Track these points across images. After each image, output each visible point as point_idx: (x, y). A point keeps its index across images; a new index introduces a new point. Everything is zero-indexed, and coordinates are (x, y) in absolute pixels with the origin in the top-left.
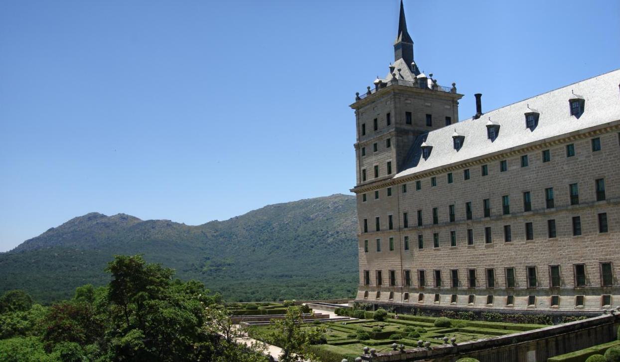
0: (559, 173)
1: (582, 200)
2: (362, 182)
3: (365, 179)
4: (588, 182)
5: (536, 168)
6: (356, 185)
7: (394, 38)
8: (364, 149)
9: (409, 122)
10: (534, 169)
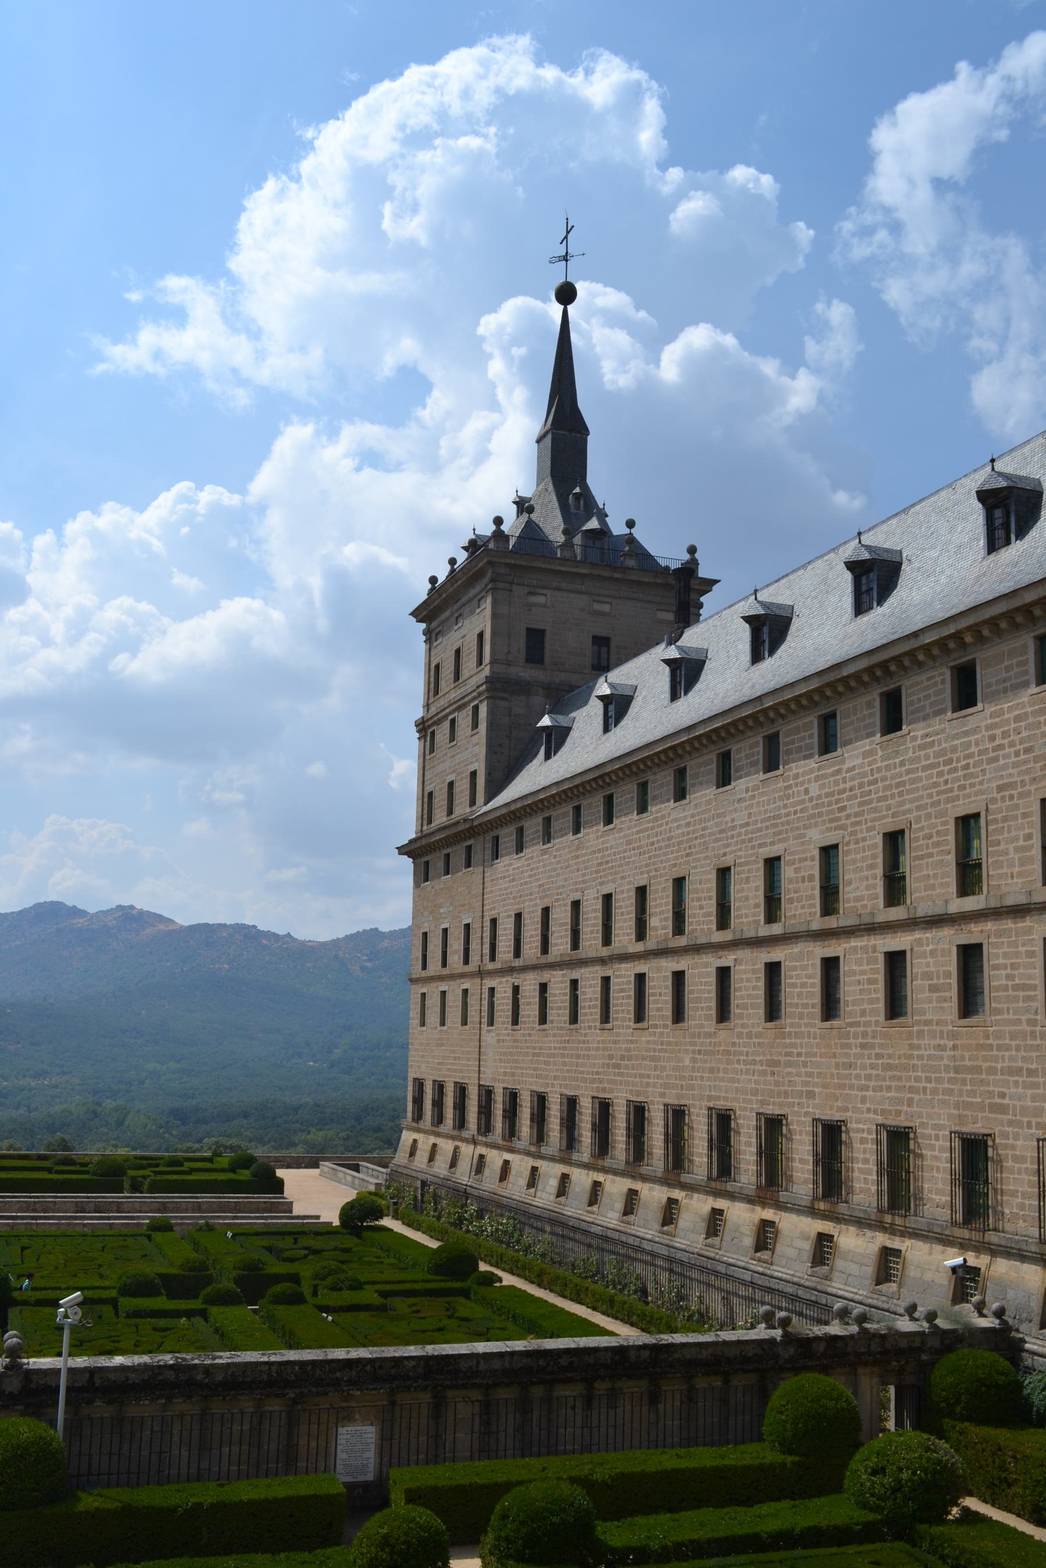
0: (798, 808)
2: (425, 828)
3: (430, 822)
4: (864, 839)
5: (747, 791)
6: (413, 836)
8: (433, 733)
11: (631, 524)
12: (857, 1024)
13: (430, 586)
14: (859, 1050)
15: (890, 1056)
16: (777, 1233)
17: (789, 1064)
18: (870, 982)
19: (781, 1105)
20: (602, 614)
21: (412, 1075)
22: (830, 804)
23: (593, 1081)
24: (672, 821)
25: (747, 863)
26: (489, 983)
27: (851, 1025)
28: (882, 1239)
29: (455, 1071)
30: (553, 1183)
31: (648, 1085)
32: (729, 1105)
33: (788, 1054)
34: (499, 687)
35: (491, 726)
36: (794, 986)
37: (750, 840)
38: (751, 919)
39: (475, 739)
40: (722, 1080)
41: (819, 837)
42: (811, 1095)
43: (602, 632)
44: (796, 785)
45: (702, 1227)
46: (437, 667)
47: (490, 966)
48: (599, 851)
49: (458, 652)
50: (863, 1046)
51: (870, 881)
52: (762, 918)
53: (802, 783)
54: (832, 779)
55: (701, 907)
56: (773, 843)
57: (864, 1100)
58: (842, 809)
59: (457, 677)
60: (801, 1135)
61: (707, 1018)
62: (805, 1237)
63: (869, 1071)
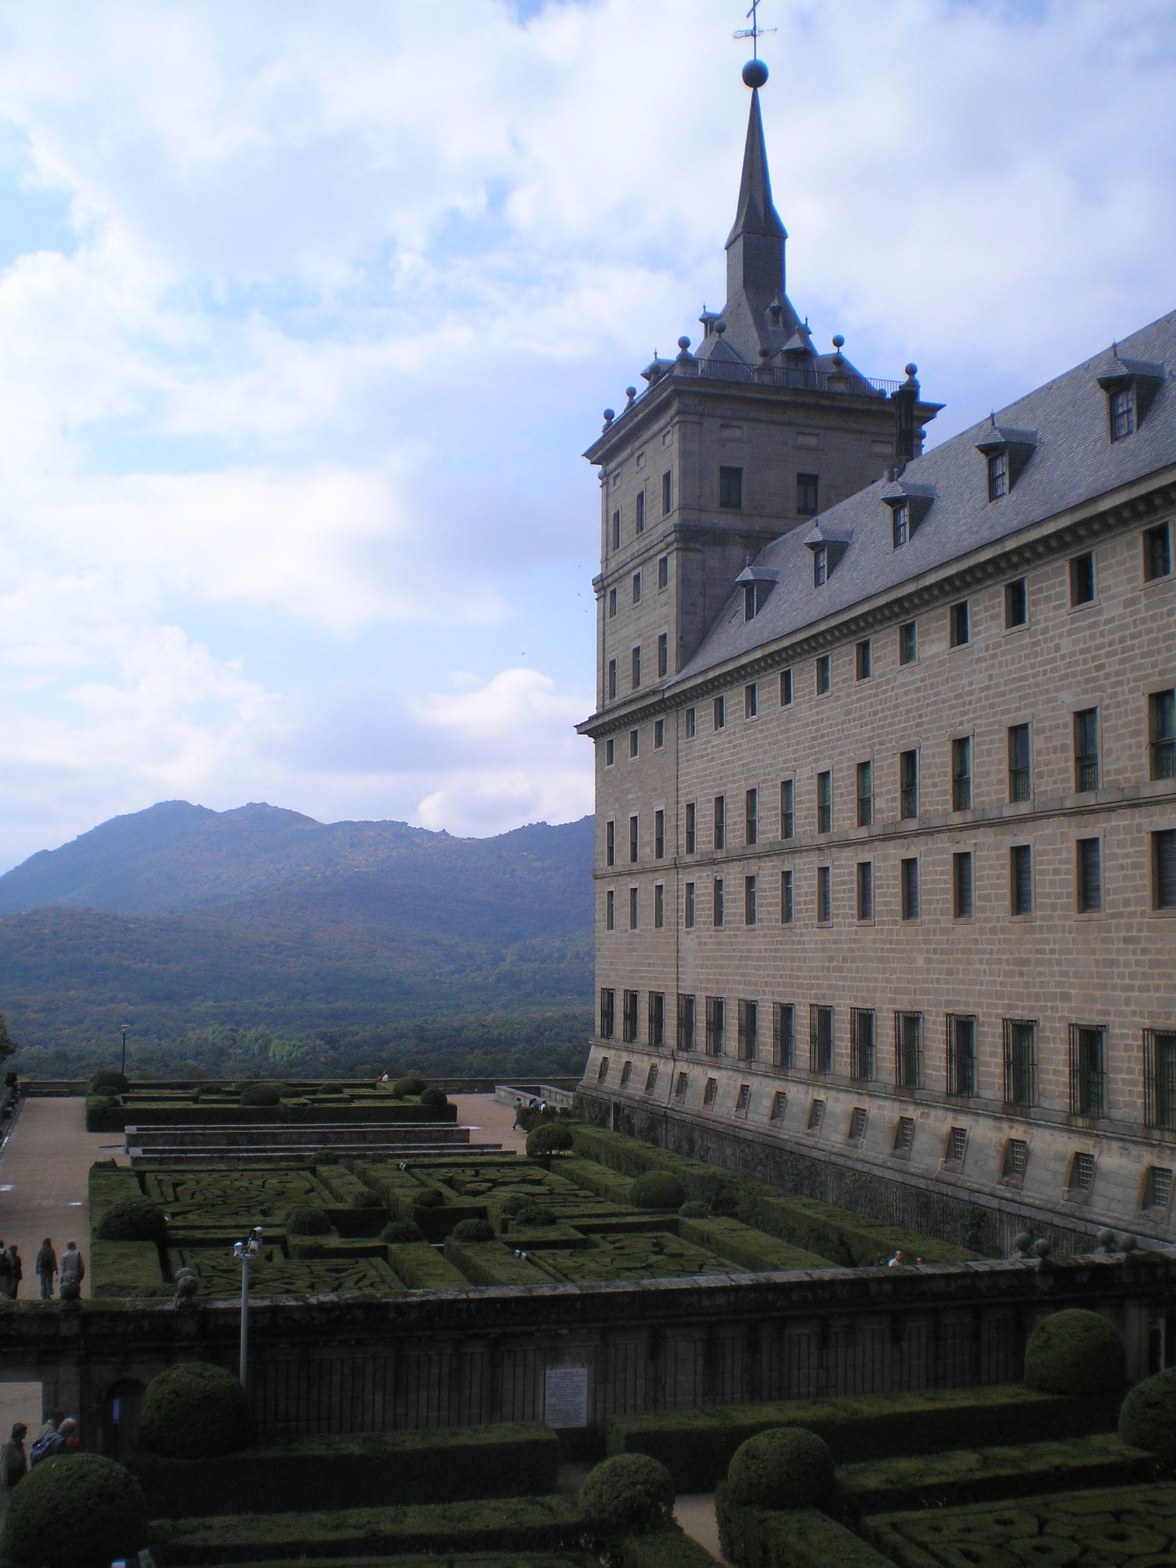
1: (1108, 773)
2: (607, 702)
4: (1126, 702)
6: (595, 712)
7: (722, 213)
8: (614, 592)
9: (731, 500)
10: (984, 654)
11: (838, 342)
12: (1120, 915)
13: (605, 421)
14: (1121, 945)
15: (1158, 951)
16: (1028, 1153)
17: (1040, 963)
18: (1135, 866)
19: (1032, 1009)
20: (808, 448)
21: (599, 986)
22: (1085, 661)
23: (811, 987)
24: (899, 687)
25: (989, 733)
26: (687, 878)
27: (1113, 916)
28: (1149, 1158)
29: (650, 979)
30: (767, 1103)
31: (875, 990)
32: (970, 1010)
33: (1038, 951)
34: (690, 536)
35: (684, 581)
36: (1043, 872)
37: (991, 706)
38: (993, 797)
39: (663, 598)
40: (962, 982)
41: (1073, 700)
42: (1066, 997)
43: (809, 470)
44: (1045, 640)
45: (941, 1148)
46: (617, 515)
47: (688, 859)
48: (813, 723)
49: (641, 497)
50: (1127, 940)
51: (1134, 750)
52: (1006, 795)
53: (1052, 639)
54: (1087, 633)
55: (935, 785)
56: (1018, 709)
57: (1128, 1001)
58: (1098, 668)
59: (640, 527)
60: (1055, 1042)
61: (944, 912)
62: (1060, 1157)
63: (1135, 969)
